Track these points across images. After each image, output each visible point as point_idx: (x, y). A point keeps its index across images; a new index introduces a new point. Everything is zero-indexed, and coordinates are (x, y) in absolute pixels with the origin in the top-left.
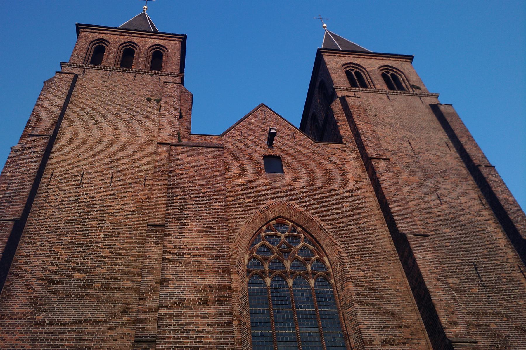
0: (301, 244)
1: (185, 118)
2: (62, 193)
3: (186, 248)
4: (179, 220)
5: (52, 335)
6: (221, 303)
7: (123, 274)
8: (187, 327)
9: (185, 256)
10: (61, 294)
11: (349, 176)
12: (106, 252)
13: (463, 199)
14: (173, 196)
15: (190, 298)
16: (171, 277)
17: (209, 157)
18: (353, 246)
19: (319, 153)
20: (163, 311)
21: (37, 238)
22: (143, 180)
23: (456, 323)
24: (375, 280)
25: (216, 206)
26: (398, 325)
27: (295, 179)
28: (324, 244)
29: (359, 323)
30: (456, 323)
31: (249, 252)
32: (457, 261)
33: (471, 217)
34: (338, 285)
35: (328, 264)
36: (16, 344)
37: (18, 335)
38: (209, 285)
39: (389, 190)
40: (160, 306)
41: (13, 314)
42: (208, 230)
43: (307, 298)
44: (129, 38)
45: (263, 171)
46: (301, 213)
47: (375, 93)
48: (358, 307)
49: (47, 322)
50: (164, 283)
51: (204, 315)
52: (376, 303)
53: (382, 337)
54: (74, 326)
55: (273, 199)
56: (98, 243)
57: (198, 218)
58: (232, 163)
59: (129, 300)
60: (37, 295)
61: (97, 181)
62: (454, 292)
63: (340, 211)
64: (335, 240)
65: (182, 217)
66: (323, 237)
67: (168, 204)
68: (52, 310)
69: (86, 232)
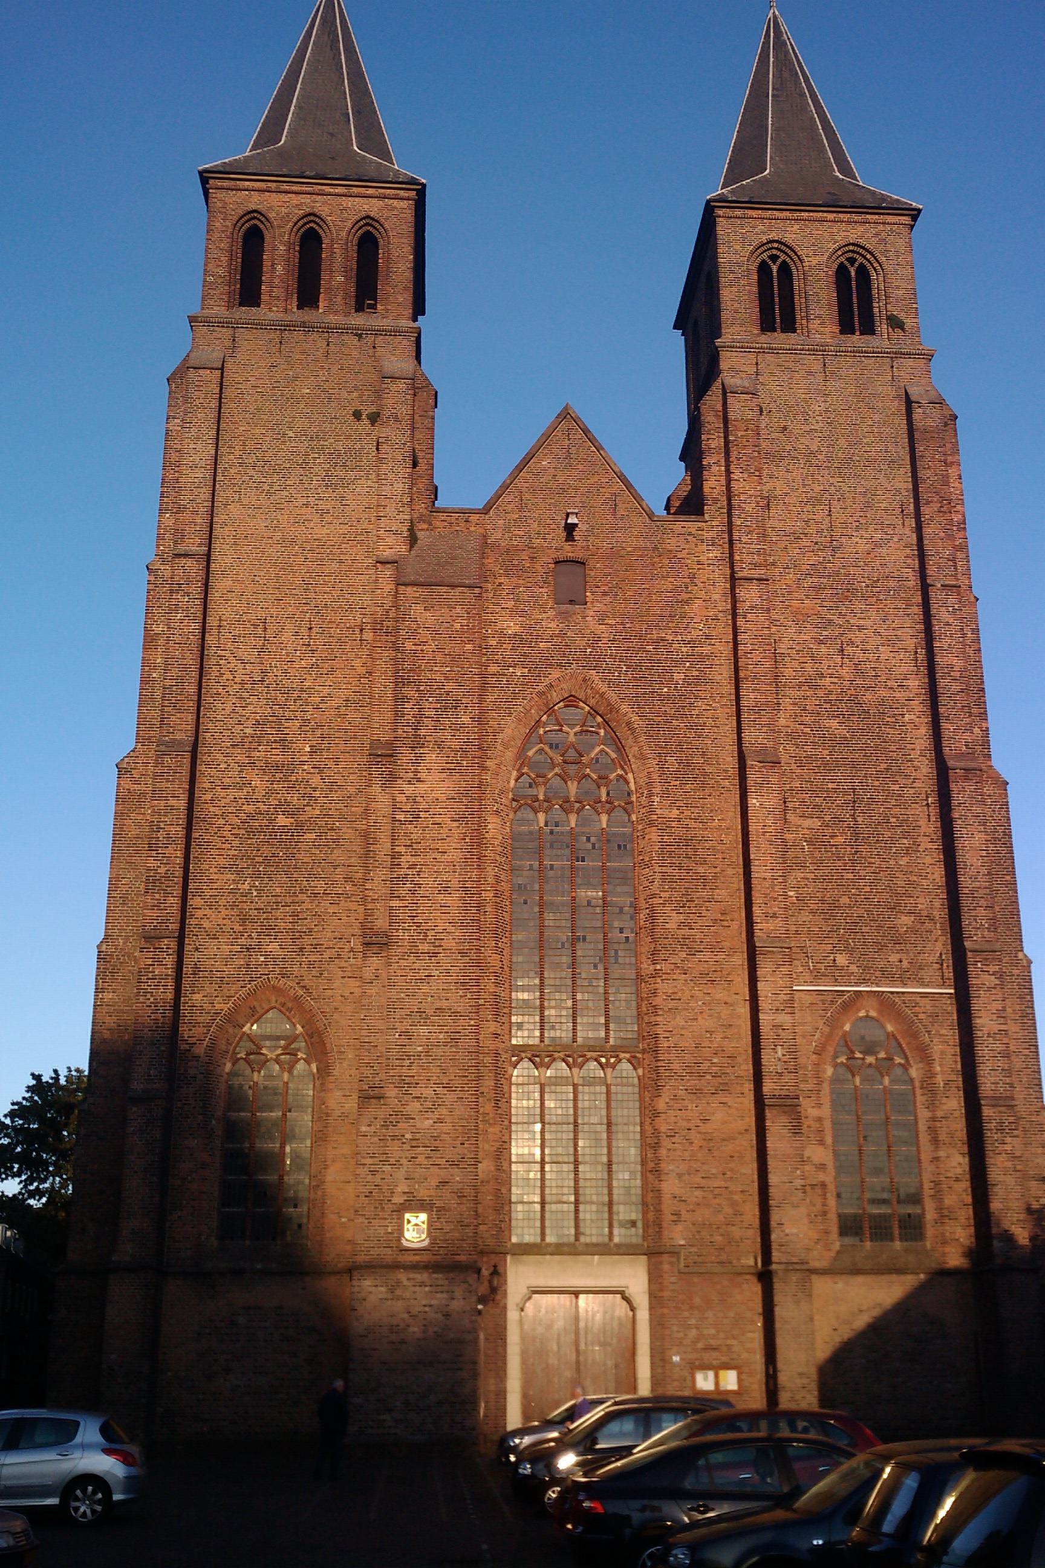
0: (598, 749)
1: (422, 466)
2: (241, 666)
3: (422, 801)
4: (413, 748)
5: (264, 913)
6: (466, 889)
7: (342, 818)
8: (424, 927)
9: (422, 814)
10: (266, 850)
11: (697, 605)
12: (316, 780)
13: (885, 652)
14: (405, 699)
15: (428, 882)
16: (403, 850)
17: (458, 609)
19: (655, 549)
20: (395, 903)
21: (220, 757)
22: (357, 631)
23: (774, 916)
24: (692, 824)
25: (466, 719)
26: (708, 898)
27: (601, 621)
28: (630, 752)
29: (653, 896)
30: (774, 916)
31: (518, 765)
32: (830, 786)
33: (884, 693)
34: (640, 827)
35: (632, 786)
36: (225, 925)
37: (224, 912)
38: (452, 862)
39: (749, 655)
40: (392, 896)
41: (212, 881)
42: (452, 766)
43: (594, 844)
44: (306, 199)
45: (551, 603)
46: (602, 695)
47: (800, 354)
48: (657, 869)
49: (255, 894)
50: (395, 855)
51: (444, 908)
52: (685, 862)
53: (681, 917)
54: (289, 900)
55: (560, 665)
56: (303, 763)
57: (439, 745)
58: (500, 584)
59: (353, 860)
60: (236, 853)
61: (287, 636)
62: (805, 844)
63: (666, 690)
64: (646, 750)
65: (417, 743)
66: (630, 741)
67: (398, 714)
68: (257, 875)
69: (283, 743)
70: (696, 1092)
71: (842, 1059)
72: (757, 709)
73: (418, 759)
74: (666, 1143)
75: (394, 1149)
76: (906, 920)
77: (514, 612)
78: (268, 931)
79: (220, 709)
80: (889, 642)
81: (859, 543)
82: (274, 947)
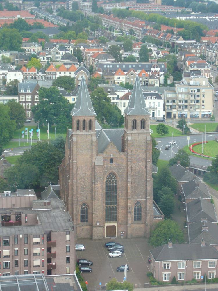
12: (87, 182)
13: (142, 166)
18: (121, 179)
27: (114, 165)
51: (100, 197)
57: (99, 181)
64: (119, 178)
69: (84, 179)
70: (122, 209)
71: (135, 205)
72: (129, 175)
73: (97, 183)
74: (119, 214)
75: (96, 217)
76: (142, 193)
77: (106, 164)
81: (141, 155)
82: (84, 198)
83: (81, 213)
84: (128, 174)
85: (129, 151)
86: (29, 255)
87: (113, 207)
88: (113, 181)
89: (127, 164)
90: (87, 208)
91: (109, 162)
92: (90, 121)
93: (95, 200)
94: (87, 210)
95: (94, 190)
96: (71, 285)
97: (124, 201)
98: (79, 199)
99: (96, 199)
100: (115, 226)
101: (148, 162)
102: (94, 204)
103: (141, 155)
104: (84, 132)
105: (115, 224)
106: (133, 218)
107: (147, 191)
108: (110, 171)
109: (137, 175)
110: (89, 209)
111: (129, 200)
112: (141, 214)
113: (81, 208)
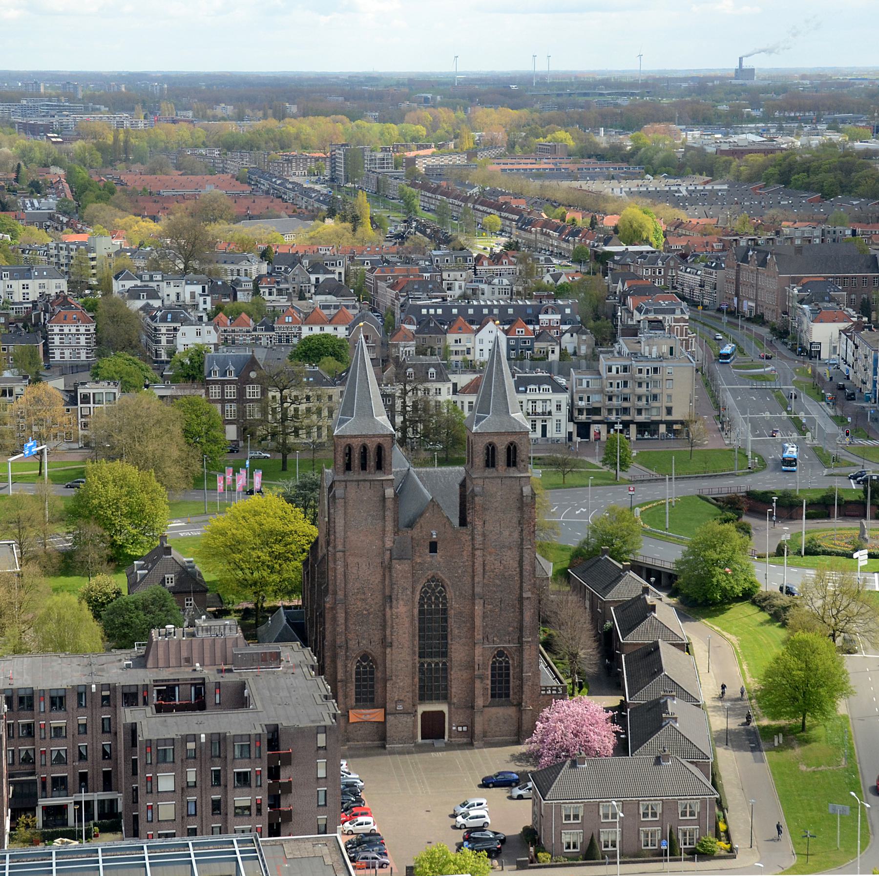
61: (364, 566)
69: (364, 593)
70: (460, 670)
77: (420, 556)
78: (363, 638)
79: (350, 586)
80: (513, 559)
83: (357, 680)
84: (476, 580)
85: (478, 523)
86: (222, 787)
87: (437, 664)
88: (437, 598)
89: (473, 555)
90: (371, 667)
91: (427, 551)
92: (380, 448)
93: (391, 646)
94: (372, 673)
95: (389, 623)
96: (328, 861)
97: (466, 648)
98: (352, 644)
99: (395, 644)
100: (442, 713)
101: (525, 551)
102: (388, 656)
103: (506, 533)
104: (362, 476)
105: (444, 708)
106: (490, 691)
107: (525, 624)
108: (430, 574)
109: (497, 581)
110: (377, 668)
111: (477, 647)
112: (508, 682)
113: (358, 667)
